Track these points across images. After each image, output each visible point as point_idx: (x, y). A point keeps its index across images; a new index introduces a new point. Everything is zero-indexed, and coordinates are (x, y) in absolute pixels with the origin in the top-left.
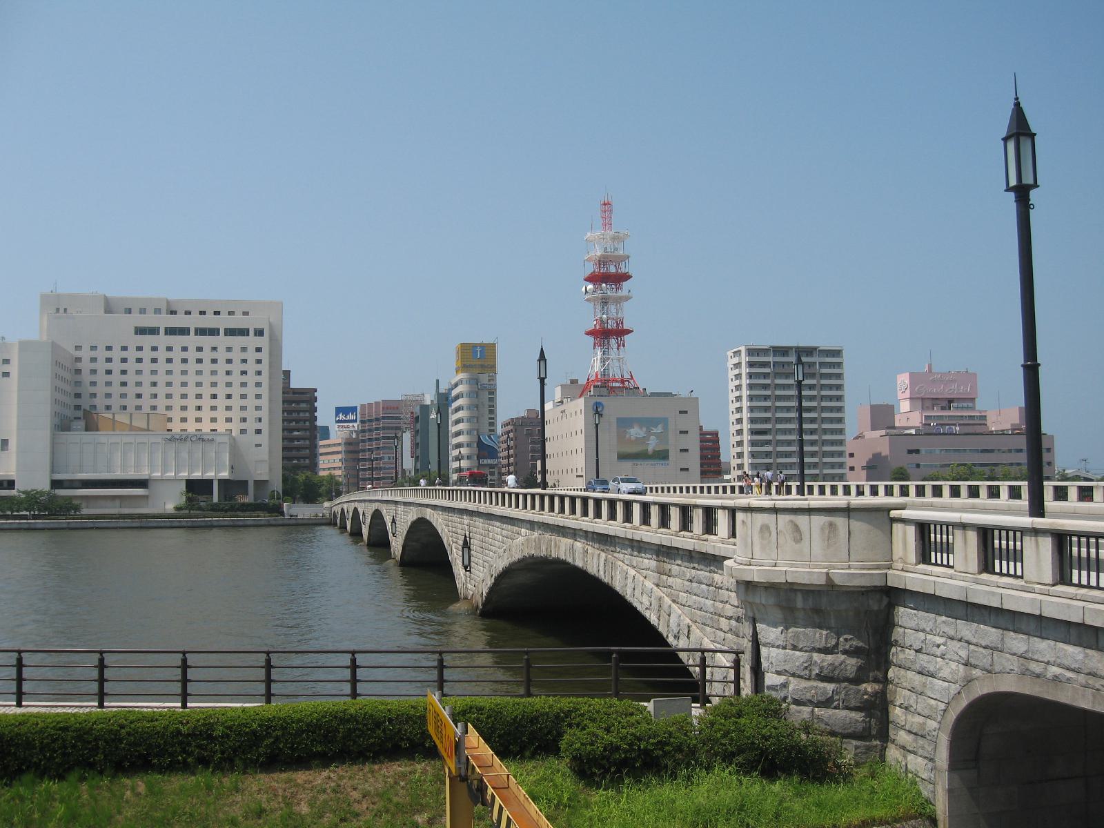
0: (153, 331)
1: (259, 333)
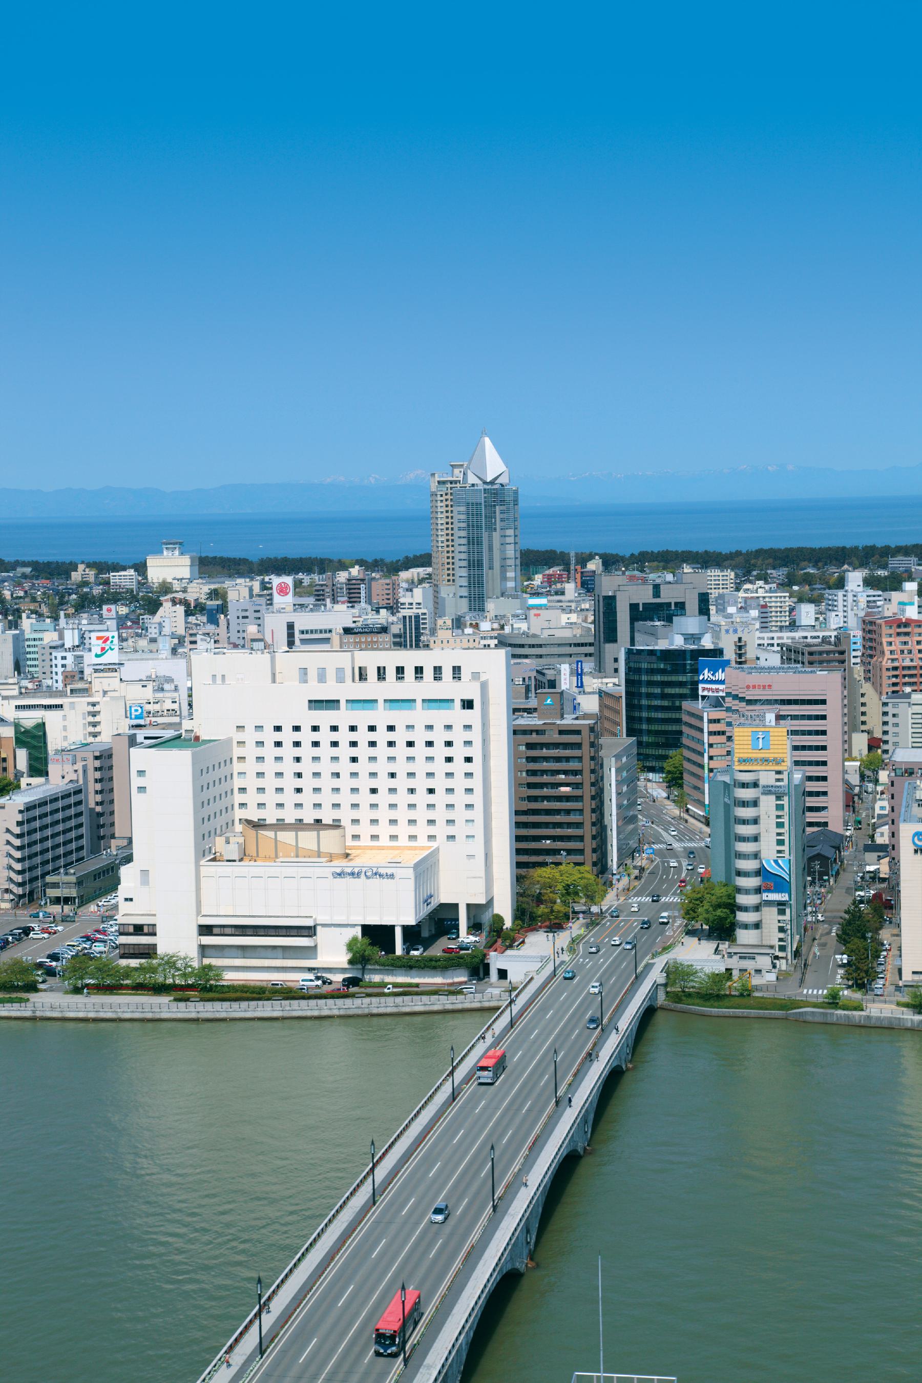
0: (332, 704)
1: (468, 704)
